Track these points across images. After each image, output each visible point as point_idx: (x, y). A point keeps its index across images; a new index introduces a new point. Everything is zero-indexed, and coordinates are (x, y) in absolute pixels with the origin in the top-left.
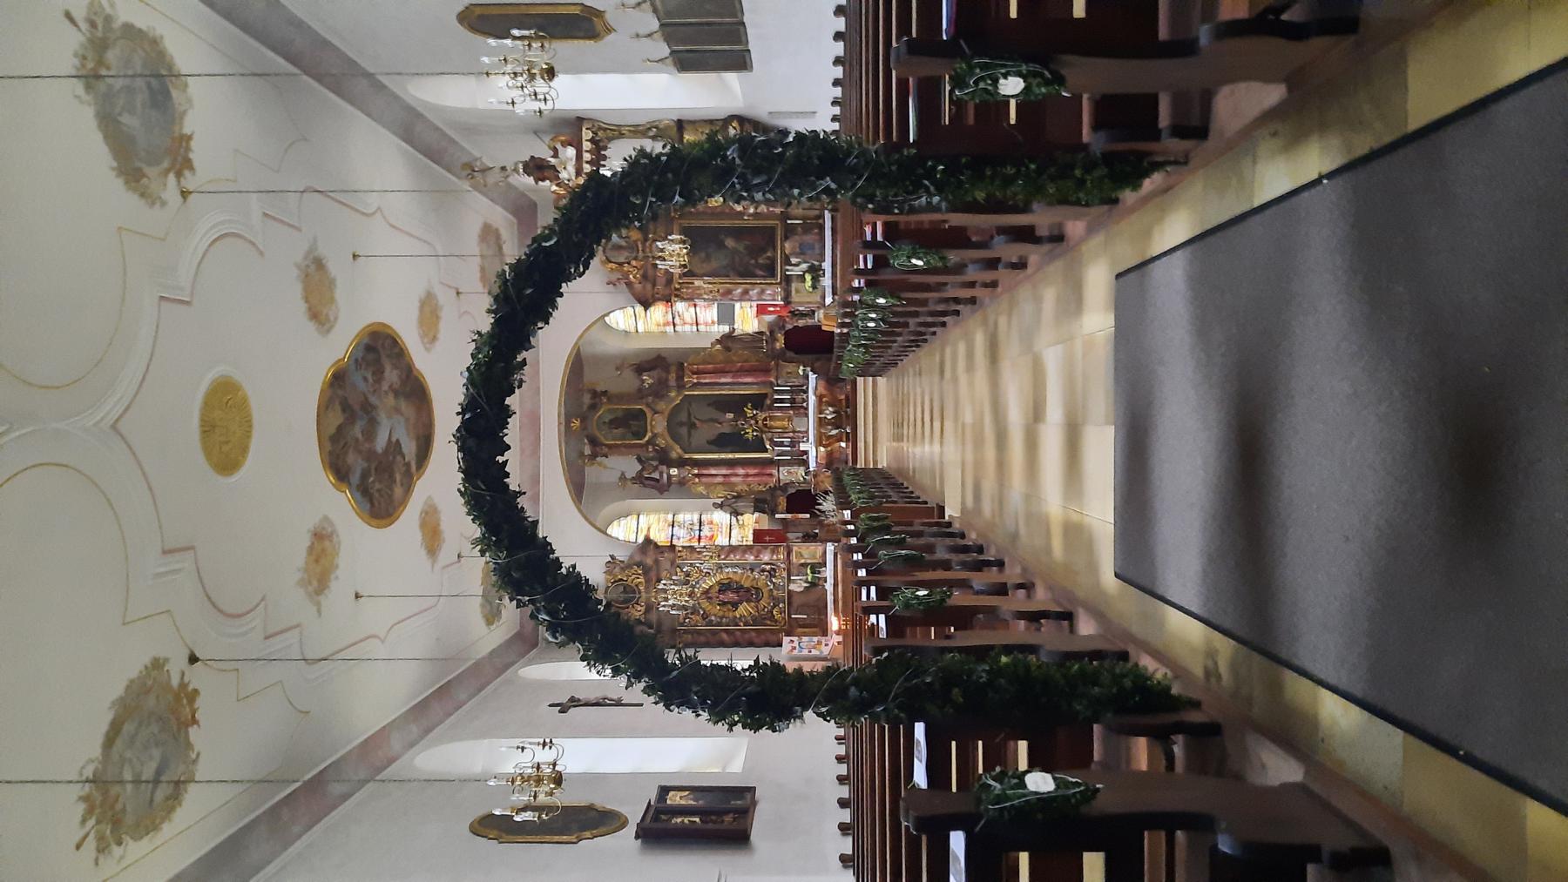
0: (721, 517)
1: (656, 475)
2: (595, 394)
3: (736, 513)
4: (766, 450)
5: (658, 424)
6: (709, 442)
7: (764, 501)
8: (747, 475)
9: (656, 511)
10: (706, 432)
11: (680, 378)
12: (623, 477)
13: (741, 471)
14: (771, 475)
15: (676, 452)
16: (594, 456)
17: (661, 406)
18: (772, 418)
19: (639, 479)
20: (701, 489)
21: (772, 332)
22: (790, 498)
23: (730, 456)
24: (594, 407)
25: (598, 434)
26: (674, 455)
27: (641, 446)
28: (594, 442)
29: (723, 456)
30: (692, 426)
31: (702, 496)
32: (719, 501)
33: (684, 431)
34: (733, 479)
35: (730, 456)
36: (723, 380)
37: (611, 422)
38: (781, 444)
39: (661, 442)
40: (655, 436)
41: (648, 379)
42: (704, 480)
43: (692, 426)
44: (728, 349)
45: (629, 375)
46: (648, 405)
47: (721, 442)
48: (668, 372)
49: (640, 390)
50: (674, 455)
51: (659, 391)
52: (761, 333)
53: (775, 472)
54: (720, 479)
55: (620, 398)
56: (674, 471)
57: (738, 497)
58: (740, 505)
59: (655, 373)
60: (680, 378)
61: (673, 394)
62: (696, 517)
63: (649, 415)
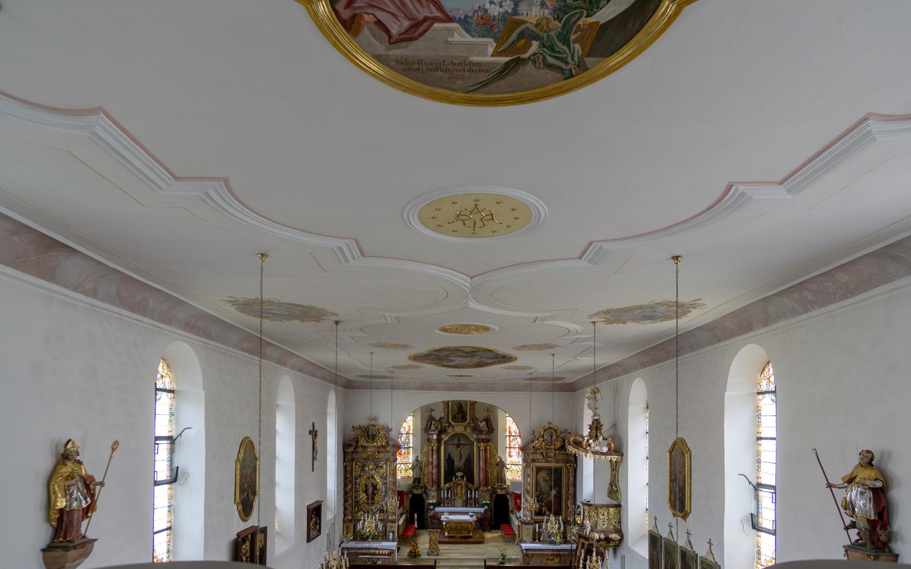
0: (411, 459)
1: (433, 428)
3: (413, 468)
4: (445, 483)
5: (459, 429)
6: (449, 455)
7: (419, 483)
9: (414, 425)
10: (455, 453)
11: (483, 441)
13: (435, 471)
15: (445, 438)
17: (469, 430)
19: (431, 419)
20: (426, 449)
23: (442, 465)
26: (443, 436)
30: (458, 446)
31: (422, 449)
33: (456, 442)
34: (430, 467)
35: (442, 465)
39: (450, 430)
40: (453, 427)
41: (483, 424)
43: (458, 446)
44: (497, 465)
47: (450, 461)
50: (443, 436)
51: (476, 429)
54: (430, 460)
56: (435, 437)
58: (418, 471)
59: (486, 429)
60: (483, 441)
62: (411, 445)
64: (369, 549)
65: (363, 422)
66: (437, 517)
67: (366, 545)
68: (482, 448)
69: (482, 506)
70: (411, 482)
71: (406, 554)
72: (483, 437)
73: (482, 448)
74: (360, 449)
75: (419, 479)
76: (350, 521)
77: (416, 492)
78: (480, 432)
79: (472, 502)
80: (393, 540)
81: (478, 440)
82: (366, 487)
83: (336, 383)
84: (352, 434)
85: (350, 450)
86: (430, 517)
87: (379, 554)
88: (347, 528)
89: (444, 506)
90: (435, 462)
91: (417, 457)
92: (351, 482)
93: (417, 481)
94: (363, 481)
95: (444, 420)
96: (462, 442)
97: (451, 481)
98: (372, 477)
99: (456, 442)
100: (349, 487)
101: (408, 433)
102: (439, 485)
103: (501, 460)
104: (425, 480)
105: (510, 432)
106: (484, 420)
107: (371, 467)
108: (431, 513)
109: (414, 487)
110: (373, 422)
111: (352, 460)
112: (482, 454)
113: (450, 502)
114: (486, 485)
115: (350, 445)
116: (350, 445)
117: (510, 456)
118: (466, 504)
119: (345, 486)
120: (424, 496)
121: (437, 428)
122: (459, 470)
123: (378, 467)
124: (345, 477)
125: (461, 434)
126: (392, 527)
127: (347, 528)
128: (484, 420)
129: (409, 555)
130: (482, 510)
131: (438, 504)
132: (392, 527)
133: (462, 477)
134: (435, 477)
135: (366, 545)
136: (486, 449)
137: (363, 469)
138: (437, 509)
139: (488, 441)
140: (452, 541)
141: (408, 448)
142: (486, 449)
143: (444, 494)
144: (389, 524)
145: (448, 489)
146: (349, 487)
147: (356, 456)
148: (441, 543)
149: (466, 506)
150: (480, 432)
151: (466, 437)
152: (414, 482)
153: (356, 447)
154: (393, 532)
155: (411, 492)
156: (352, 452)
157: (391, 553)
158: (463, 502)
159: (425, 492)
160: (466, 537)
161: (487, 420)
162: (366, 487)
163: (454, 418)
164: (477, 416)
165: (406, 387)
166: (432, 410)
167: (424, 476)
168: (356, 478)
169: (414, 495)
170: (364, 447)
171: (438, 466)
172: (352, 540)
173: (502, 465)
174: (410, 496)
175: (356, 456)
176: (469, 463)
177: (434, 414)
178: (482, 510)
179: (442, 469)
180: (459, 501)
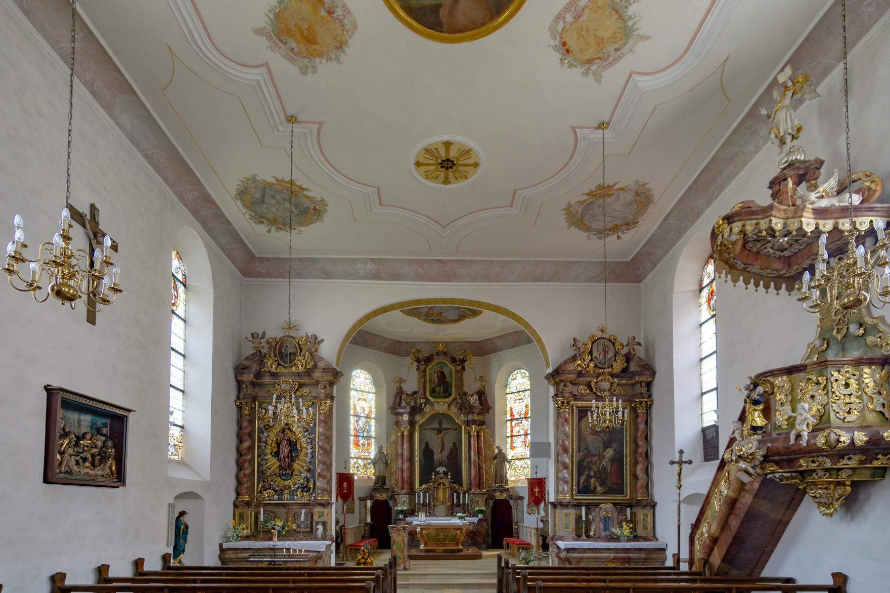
0: (373, 453)
2: (463, 361)
3: (375, 463)
4: (421, 485)
5: (440, 406)
7: (384, 483)
8: (402, 471)
11: (474, 422)
12: (401, 381)
13: (406, 466)
14: (403, 488)
15: (420, 419)
16: (418, 360)
17: (454, 409)
18: (445, 489)
19: (400, 392)
20: (393, 437)
21: (507, 490)
22: (385, 502)
23: (417, 459)
24: (453, 360)
25: (434, 363)
27: (425, 394)
28: (428, 360)
29: (417, 453)
30: (439, 431)
31: (388, 437)
32: (384, 450)
33: (436, 425)
34: (400, 461)
35: (417, 459)
36: (472, 454)
37: (443, 373)
38: (425, 497)
39: (427, 409)
40: (432, 405)
41: (474, 400)
42: (400, 440)
43: (439, 431)
44: (495, 458)
45: (477, 386)
46: (455, 399)
47: (427, 452)
48: (478, 414)
49: (465, 394)
50: (418, 418)
51: (466, 408)
52: (507, 483)
53: (405, 491)
54: (400, 451)
55: (460, 380)
56: (406, 417)
57: (387, 464)
58: (382, 466)
60: (474, 422)
61: (462, 417)
62: (373, 434)
63: (447, 400)
70: (372, 484)
72: (475, 417)
75: (384, 478)
76: (248, 504)
77: (379, 496)
78: (469, 410)
81: (468, 423)
90: (406, 454)
92: (251, 435)
93: (381, 481)
95: (420, 395)
96: (444, 426)
99: (436, 425)
100: (246, 444)
101: (368, 417)
104: (390, 483)
105: (512, 415)
109: (375, 489)
112: (473, 442)
117: (513, 448)
120: (391, 503)
122: (441, 465)
133: (445, 474)
134: (406, 474)
136: (478, 436)
139: (482, 423)
141: (369, 437)
142: (478, 436)
143: (419, 499)
146: (246, 444)
152: (376, 483)
155: (371, 497)
159: (392, 497)
160: (452, 551)
161: (481, 394)
164: (466, 390)
171: (411, 460)
173: (501, 458)
176: (455, 454)
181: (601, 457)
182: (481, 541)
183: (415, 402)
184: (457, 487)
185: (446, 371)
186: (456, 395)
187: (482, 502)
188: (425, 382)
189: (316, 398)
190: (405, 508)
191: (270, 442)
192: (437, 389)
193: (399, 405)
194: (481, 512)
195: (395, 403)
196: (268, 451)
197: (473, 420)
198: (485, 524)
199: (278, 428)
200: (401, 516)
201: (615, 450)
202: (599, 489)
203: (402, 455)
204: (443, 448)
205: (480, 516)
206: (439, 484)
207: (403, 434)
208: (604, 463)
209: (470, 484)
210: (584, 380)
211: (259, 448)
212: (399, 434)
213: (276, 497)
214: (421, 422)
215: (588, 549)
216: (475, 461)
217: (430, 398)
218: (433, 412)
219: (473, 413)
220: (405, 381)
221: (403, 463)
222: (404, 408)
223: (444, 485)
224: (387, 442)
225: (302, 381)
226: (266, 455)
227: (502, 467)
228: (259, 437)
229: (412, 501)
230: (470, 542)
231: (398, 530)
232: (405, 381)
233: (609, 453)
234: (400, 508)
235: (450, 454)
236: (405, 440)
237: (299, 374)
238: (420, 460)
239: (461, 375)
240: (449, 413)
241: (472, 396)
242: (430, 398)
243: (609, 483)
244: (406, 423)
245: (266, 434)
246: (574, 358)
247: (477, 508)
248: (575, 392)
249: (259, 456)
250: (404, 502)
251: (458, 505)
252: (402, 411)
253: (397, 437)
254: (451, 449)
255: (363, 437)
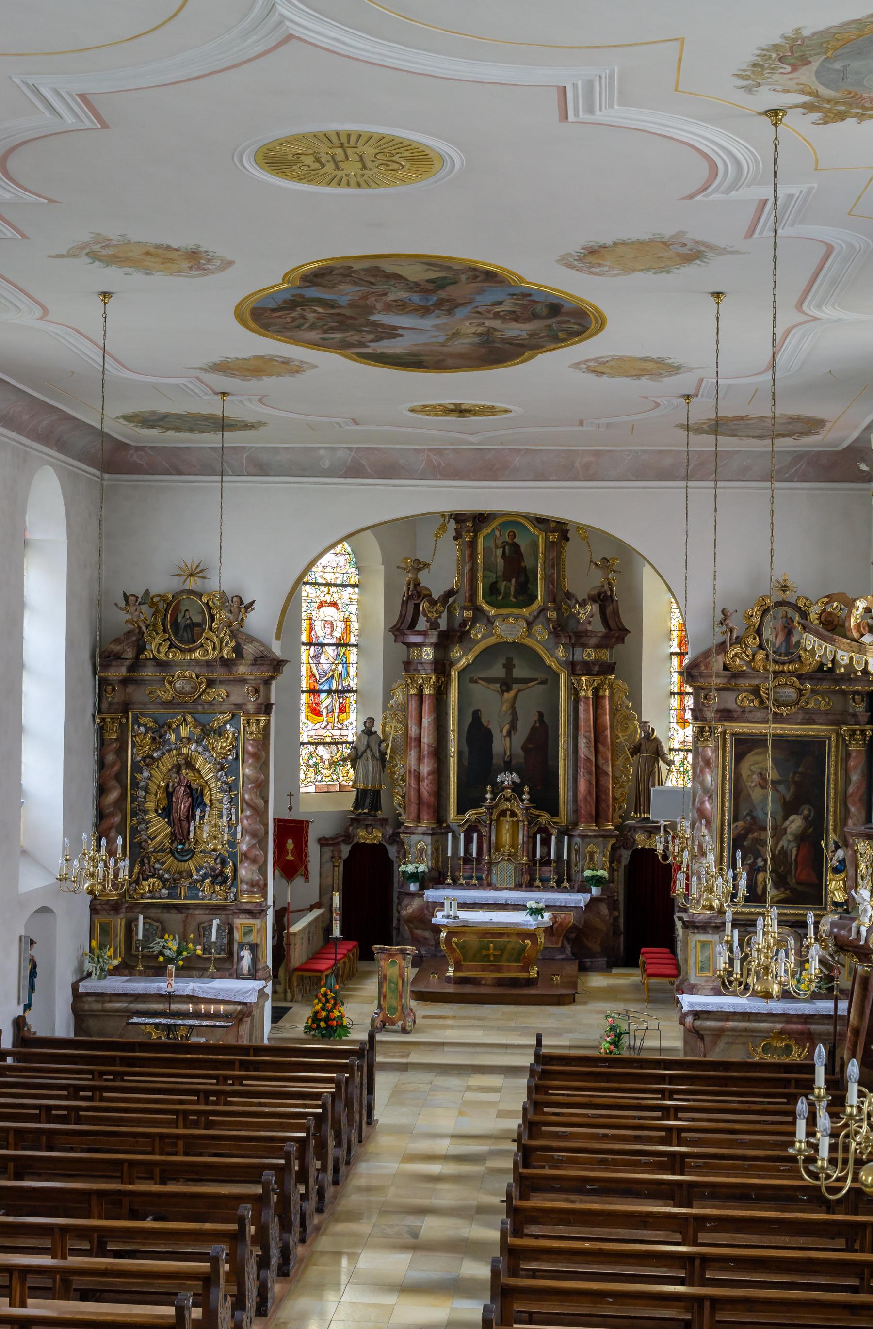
0: (351, 729)
1: (422, 624)
3: (355, 759)
4: (461, 811)
5: (508, 627)
6: (476, 715)
7: (376, 805)
10: (494, 707)
11: (587, 668)
13: (425, 769)
14: (418, 819)
15: (462, 658)
17: (541, 632)
18: (515, 825)
23: (453, 749)
26: (456, 652)
27: (472, 598)
29: (453, 737)
30: (506, 684)
31: (388, 695)
32: (378, 728)
33: (498, 671)
34: (413, 754)
35: (453, 749)
36: (582, 743)
37: (516, 547)
38: (468, 841)
39: (478, 632)
40: (490, 622)
41: (588, 613)
42: (413, 704)
43: (506, 684)
44: (636, 750)
45: (595, 580)
46: (542, 610)
47: (477, 735)
48: (598, 647)
53: (424, 826)
54: (413, 731)
58: (369, 764)
59: (597, 626)
60: (587, 668)
63: (525, 611)
64: (169, 997)
65: (163, 584)
66: (423, 918)
67: (161, 986)
68: (586, 692)
69: (583, 889)
70: (348, 803)
71: (301, 1027)
72: (589, 655)
73: (586, 692)
74: (149, 672)
75: (376, 794)
77: (364, 836)
78: (578, 639)
79: (549, 872)
80: (253, 975)
81: (573, 668)
82: (170, 795)
83: (61, 446)
84: (121, 619)
85: (119, 672)
86: (410, 920)
87: (197, 1015)
88: (105, 930)
89: (455, 884)
90: (427, 739)
91: (371, 720)
93: (368, 800)
94: (157, 778)
97: (477, 802)
98: (190, 764)
99: (498, 671)
102: (440, 817)
103: (649, 736)
104: (394, 801)
106: (593, 599)
107: (184, 732)
108: (411, 907)
109: (356, 821)
110: (192, 584)
111: (126, 707)
112: (585, 714)
113: (474, 870)
114: (598, 817)
115: (118, 657)
116: (118, 657)
118: (528, 880)
119: (102, 790)
121: (434, 625)
122: (508, 767)
123: (206, 731)
124: (101, 764)
125: (516, 646)
126: (248, 931)
127: (105, 930)
128: (593, 599)
129: (308, 1028)
130: (580, 899)
131: (436, 878)
132: (248, 931)
133: (517, 788)
135: (161, 986)
136: (597, 698)
137: (159, 740)
138: (431, 895)
139: (607, 669)
140: (468, 993)
141: (343, 692)
142: (597, 698)
143: (455, 846)
144: (240, 921)
145: (471, 829)
147: (138, 694)
148: (422, 997)
149: (530, 886)
150: (578, 639)
151: (534, 658)
152: (357, 804)
153: (134, 667)
154: (254, 948)
155: (347, 837)
156: (125, 682)
157: (243, 1013)
158: (519, 871)
161: (603, 599)
162: (170, 795)
163: (492, 591)
165: (302, 466)
166: (419, 566)
167: (393, 783)
168: (137, 769)
169: (359, 849)
170: (162, 665)
171: (439, 753)
172: (116, 971)
174: (346, 850)
175: (138, 694)
176: (541, 740)
177: (424, 578)
178: (580, 899)
179: (453, 762)
180: (504, 871)
181: (779, 832)
182: (597, 948)
183: (451, 616)
184: (544, 818)
185: (523, 543)
186: (545, 600)
187: (602, 857)
188: (473, 571)
189: (239, 706)
190: (422, 868)
191: (153, 788)
192: (503, 585)
193: (413, 625)
194: (598, 881)
195: (402, 617)
196: (150, 805)
197: (586, 664)
198: (604, 910)
199: (168, 762)
200: (413, 887)
201: (806, 818)
202: (771, 892)
203: (419, 740)
204: (513, 727)
205: (595, 891)
206: (503, 813)
207: (420, 695)
208: (783, 843)
209: (576, 811)
210: (743, 683)
211: (134, 798)
212: (413, 692)
213: (164, 891)
214: (463, 662)
215: (734, 1013)
216: (588, 760)
217: (486, 607)
218: (492, 640)
219: (584, 646)
220: (426, 565)
221: (420, 759)
222: (424, 634)
223: (513, 814)
224: (385, 707)
225: (214, 676)
226: (146, 812)
227: (651, 773)
228: (133, 778)
229: (439, 850)
230: (568, 950)
231: (391, 955)
232: (426, 565)
233: (795, 824)
234: (410, 868)
235: (529, 739)
236: (426, 707)
237: (208, 664)
238: (460, 753)
239: (559, 553)
240: (529, 642)
241: (583, 604)
242: (486, 607)
243: (792, 882)
244: (429, 668)
245: (146, 774)
246: (722, 647)
247: (588, 873)
248: (731, 705)
249: (134, 814)
250: (421, 851)
251: (546, 862)
252: (418, 639)
253: (408, 697)
254: (534, 728)
255: (329, 692)
